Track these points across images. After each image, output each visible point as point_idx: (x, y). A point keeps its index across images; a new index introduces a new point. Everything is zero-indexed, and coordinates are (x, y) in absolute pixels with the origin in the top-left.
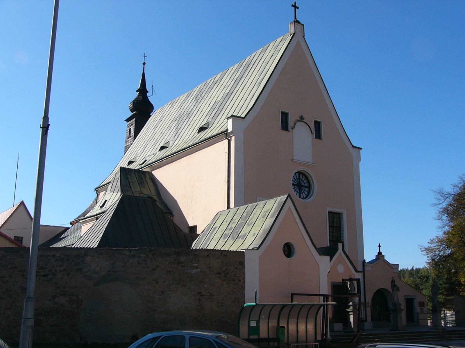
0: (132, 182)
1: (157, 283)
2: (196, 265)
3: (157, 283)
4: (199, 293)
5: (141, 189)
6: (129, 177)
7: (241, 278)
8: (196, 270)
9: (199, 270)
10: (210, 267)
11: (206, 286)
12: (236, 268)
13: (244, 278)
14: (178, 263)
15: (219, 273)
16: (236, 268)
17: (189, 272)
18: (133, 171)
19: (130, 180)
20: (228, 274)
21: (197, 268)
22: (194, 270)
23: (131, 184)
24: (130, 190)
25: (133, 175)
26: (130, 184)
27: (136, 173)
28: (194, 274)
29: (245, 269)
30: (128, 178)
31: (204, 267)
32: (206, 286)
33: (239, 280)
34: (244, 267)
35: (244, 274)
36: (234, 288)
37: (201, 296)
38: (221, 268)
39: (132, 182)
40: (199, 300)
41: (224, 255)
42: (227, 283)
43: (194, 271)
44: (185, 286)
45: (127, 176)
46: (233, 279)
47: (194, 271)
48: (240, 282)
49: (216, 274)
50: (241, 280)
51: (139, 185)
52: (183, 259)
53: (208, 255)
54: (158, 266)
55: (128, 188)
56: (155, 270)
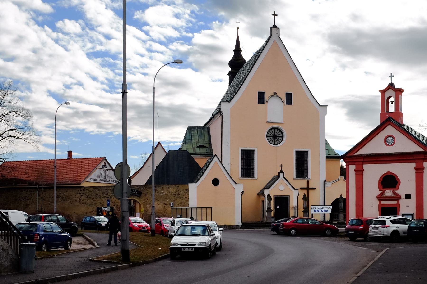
0: (194, 136)
1: (148, 200)
2: (163, 191)
3: (148, 200)
4: (164, 203)
5: (199, 140)
6: (192, 132)
7: (187, 197)
8: (163, 194)
10: (170, 192)
11: (168, 200)
15: (175, 195)
17: (160, 194)
18: (197, 128)
19: (193, 135)
20: (180, 195)
21: (163, 193)
23: (193, 137)
24: (191, 141)
26: (192, 138)
27: (198, 129)
30: (191, 133)
31: (167, 192)
32: (168, 200)
33: (186, 198)
35: (188, 195)
36: (183, 201)
37: (166, 205)
39: (194, 136)
40: (165, 206)
41: (177, 187)
43: (162, 194)
44: (158, 200)
45: (191, 132)
47: (162, 194)
48: (186, 198)
49: (173, 195)
50: (186, 197)
51: (198, 137)
52: (158, 189)
53: (168, 187)
54: (147, 193)
55: (189, 141)
56: (147, 194)
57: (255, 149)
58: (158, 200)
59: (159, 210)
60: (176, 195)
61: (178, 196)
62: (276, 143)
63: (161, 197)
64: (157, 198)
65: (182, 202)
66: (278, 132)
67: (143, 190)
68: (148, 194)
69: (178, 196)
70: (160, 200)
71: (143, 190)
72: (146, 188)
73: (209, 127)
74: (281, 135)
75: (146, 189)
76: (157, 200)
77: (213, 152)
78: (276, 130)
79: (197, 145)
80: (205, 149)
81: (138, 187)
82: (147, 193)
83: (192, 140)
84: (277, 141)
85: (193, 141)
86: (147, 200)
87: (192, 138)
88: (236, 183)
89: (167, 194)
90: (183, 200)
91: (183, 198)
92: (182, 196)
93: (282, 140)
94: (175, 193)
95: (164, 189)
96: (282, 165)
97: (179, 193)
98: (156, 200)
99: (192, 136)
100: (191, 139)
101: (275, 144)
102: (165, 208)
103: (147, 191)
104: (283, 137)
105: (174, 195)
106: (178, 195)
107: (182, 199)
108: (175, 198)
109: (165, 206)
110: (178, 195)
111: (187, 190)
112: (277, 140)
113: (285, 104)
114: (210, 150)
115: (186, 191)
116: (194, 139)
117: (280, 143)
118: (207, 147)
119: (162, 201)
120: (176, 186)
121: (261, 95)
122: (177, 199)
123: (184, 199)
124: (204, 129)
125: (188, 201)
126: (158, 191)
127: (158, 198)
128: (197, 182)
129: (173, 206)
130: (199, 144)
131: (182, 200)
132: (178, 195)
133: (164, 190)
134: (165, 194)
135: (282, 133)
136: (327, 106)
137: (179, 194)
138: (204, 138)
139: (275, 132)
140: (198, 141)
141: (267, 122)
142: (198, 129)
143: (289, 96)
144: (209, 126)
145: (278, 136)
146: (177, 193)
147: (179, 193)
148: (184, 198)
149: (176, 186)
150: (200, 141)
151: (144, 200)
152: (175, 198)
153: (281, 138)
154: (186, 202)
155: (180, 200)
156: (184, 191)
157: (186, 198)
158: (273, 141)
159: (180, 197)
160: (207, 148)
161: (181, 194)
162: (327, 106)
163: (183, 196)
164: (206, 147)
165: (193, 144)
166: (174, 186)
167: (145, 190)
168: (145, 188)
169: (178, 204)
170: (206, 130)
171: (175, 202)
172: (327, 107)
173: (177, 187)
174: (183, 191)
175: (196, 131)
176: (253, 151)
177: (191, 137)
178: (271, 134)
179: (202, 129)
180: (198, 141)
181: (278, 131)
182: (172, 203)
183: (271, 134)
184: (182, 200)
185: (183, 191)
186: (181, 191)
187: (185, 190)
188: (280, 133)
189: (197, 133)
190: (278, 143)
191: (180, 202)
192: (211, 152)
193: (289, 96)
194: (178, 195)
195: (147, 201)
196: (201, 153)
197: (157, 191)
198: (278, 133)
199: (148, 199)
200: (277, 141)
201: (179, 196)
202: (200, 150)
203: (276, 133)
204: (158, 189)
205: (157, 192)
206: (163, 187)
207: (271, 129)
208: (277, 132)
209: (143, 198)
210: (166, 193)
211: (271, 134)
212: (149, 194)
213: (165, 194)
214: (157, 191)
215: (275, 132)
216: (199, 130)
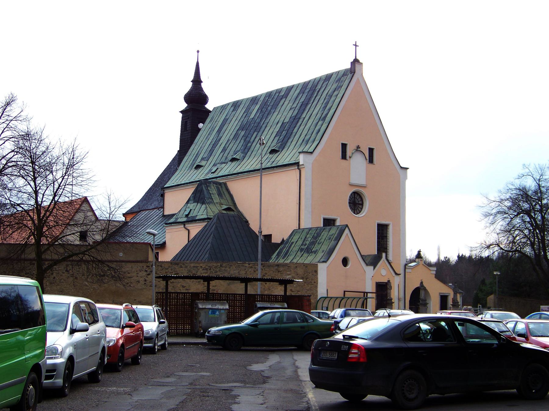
2: (289, 273)
4: (291, 290)
6: (209, 189)
7: (315, 281)
8: (290, 276)
10: (297, 274)
11: (295, 286)
14: (278, 272)
19: (211, 192)
20: (308, 278)
21: (289, 275)
23: (212, 195)
31: (294, 274)
33: (315, 282)
35: (317, 278)
38: (304, 275)
39: (213, 194)
42: (307, 284)
52: (282, 269)
53: (296, 267)
57: (337, 219)
62: (356, 213)
65: (310, 289)
74: (360, 202)
75: (264, 269)
78: (356, 195)
82: (266, 274)
83: (212, 199)
86: (265, 284)
92: (311, 281)
93: (362, 209)
94: (304, 275)
95: (292, 270)
100: (211, 198)
101: (355, 214)
103: (266, 272)
104: (362, 204)
107: (310, 284)
111: (316, 272)
115: (315, 274)
122: (305, 284)
123: (312, 285)
126: (281, 273)
133: (291, 271)
135: (362, 200)
136: (408, 168)
138: (226, 199)
145: (358, 203)
146: (305, 275)
148: (313, 283)
153: (360, 206)
154: (315, 288)
157: (315, 282)
159: (308, 281)
163: (312, 280)
169: (306, 291)
171: (303, 288)
177: (209, 195)
187: (314, 272)
189: (214, 189)
191: (308, 288)
197: (281, 272)
201: (308, 279)
205: (281, 274)
206: (289, 267)
208: (356, 198)
211: (351, 200)
214: (281, 272)
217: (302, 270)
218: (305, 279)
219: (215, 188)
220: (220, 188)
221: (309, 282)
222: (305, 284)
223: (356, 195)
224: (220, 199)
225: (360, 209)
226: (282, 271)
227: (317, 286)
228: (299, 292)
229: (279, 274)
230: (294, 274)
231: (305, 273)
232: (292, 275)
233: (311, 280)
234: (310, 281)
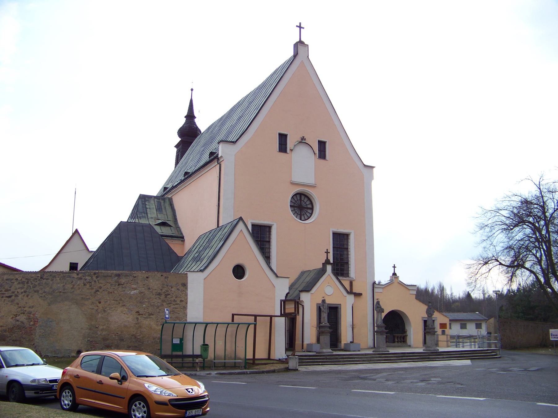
0: (150, 208)
1: (100, 303)
2: (135, 286)
4: (138, 312)
7: (183, 299)
9: (138, 291)
10: (149, 289)
11: (144, 306)
12: (178, 289)
13: (187, 299)
14: (119, 285)
15: (160, 294)
16: (178, 289)
18: (153, 198)
19: (147, 207)
20: (169, 295)
21: (135, 289)
22: (133, 291)
23: (148, 210)
25: (152, 202)
26: (146, 211)
27: (156, 200)
28: (132, 295)
29: (187, 290)
31: (144, 289)
32: (144, 306)
33: (181, 301)
34: (187, 288)
35: (187, 295)
36: (176, 308)
37: (139, 315)
38: (161, 290)
39: (150, 208)
40: (137, 318)
43: (132, 293)
44: (124, 305)
46: (174, 300)
47: (132, 293)
48: (182, 302)
49: (156, 295)
50: (183, 301)
51: (156, 210)
52: (124, 281)
53: (147, 277)
54: (100, 288)
55: (143, 215)
56: (98, 291)
57: (273, 225)
58: (124, 303)
59: (125, 326)
60: (163, 297)
61: (166, 297)
62: (303, 218)
63: (131, 297)
64: (121, 300)
66: (305, 201)
67: (90, 283)
68: (100, 290)
69: (166, 297)
70: (128, 305)
71: (90, 283)
72: (97, 277)
73: (172, 198)
74: (310, 206)
75: (98, 280)
76: (121, 305)
77: (182, 234)
78: (303, 197)
79: (155, 222)
80: (169, 228)
81: (79, 276)
82: (100, 288)
83: (147, 213)
84: (303, 215)
85: (149, 216)
86: (98, 303)
87: (148, 212)
88: (277, 276)
89: (142, 293)
90: (176, 306)
91: (176, 301)
92: (174, 298)
93: (311, 214)
94: (161, 290)
95: (139, 282)
96: (329, 251)
97: (167, 291)
98: (119, 303)
99: (146, 208)
100: (146, 212)
101: (301, 219)
102: (139, 321)
104: (312, 209)
105: (158, 295)
106: (165, 295)
107: (174, 303)
108: (160, 301)
109: (139, 317)
110: (166, 296)
111: (185, 285)
112: (304, 213)
113: (318, 157)
114: (178, 231)
115: (182, 288)
116: (151, 214)
117: (309, 218)
118: (172, 227)
119: (132, 307)
120: (162, 275)
121: (283, 138)
122: (164, 304)
123: (177, 304)
124: (164, 200)
125: (185, 308)
126: (123, 286)
127: (123, 299)
128: (204, 270)
129: (168, 318)
130: (160, 221)
131: (174, 306)
132: (166, 296)
133: (137, 283)
134: (141, 293)
135: (311, 203)
137: (168, 293)
138: (165, 213)
139: (301, 200)
140: (156, 216)
141: (291, 183)
142: (155, 199)
143: (322, 145)
144: (172, 197)
145: (306, 206)
146: (163, 291)
147: (168, 291)
148: (178, 302)
149: (162, 275)
150: (160, 216)
151: (93, 303)
152: (160, 301)
153: (310, 211)
154: (182, 310)
155: (169, 305)
156: (178, 287)
157: (181, 301)
158: (298, 214)
160: (171, 227)
161: (173, 294)
162: (373, 167)
163: (176, 297)
164: (170, 226)
165: (149, 220)
166: (159, 274)
167: (95, 282)
168: (94, 278)
170: (167, 201)
172: (374, 169)
173: (165, 278)
174: (175, 288)
175: (152, 202)
176: (269, 227)
177: (145, 209)
178: (297, 202)
179: (161, 200)
180: (157, 216)
181: (306, 200)
182: (167, 310)
183: (295, 203)
184: (174, 306)
185: (176, 287)
186: (172, 287)
187: (181, 285)
188: (308, 203)
189: (154, 204)
190: (306, 218)
192: (180, 233)
193: (322, 145)
194: (165, 295)
195: (99, 305)
196: (164, 234)
198: (305, 203)
199: (102, 301)
200: (303, 215)
202: (161, 229)
203: (302, 202)
204: (123, 280)
205: (123, 287)
206: (135, 277)
207: (296, 195)
208: (304, 201)
209: (89, 298)
210: (143, 290)
212: (103, 292)
213: (141, 293)
214: (122, 285)
215: (301, 200)
216: (157, 201)
217: (157, 282)
218: (165, 296)
219: (156, 202)
220: (162, 204)
221: (171, 300)
222: (164, 304)
223: (303, 197)
224: (158, 214)
225: (309, 215)
226: (124, 283)
227: (187, 306)
228: (153, 315)
229: (120, 289)
230: (143, 287)
231: (163, 287)
232: (140, 289)
233: (174, 298)
234: (173, 299)
